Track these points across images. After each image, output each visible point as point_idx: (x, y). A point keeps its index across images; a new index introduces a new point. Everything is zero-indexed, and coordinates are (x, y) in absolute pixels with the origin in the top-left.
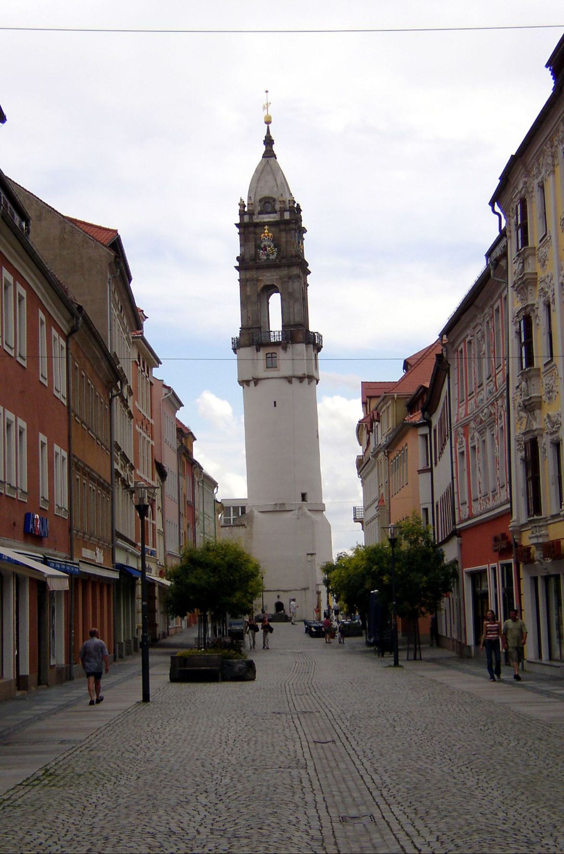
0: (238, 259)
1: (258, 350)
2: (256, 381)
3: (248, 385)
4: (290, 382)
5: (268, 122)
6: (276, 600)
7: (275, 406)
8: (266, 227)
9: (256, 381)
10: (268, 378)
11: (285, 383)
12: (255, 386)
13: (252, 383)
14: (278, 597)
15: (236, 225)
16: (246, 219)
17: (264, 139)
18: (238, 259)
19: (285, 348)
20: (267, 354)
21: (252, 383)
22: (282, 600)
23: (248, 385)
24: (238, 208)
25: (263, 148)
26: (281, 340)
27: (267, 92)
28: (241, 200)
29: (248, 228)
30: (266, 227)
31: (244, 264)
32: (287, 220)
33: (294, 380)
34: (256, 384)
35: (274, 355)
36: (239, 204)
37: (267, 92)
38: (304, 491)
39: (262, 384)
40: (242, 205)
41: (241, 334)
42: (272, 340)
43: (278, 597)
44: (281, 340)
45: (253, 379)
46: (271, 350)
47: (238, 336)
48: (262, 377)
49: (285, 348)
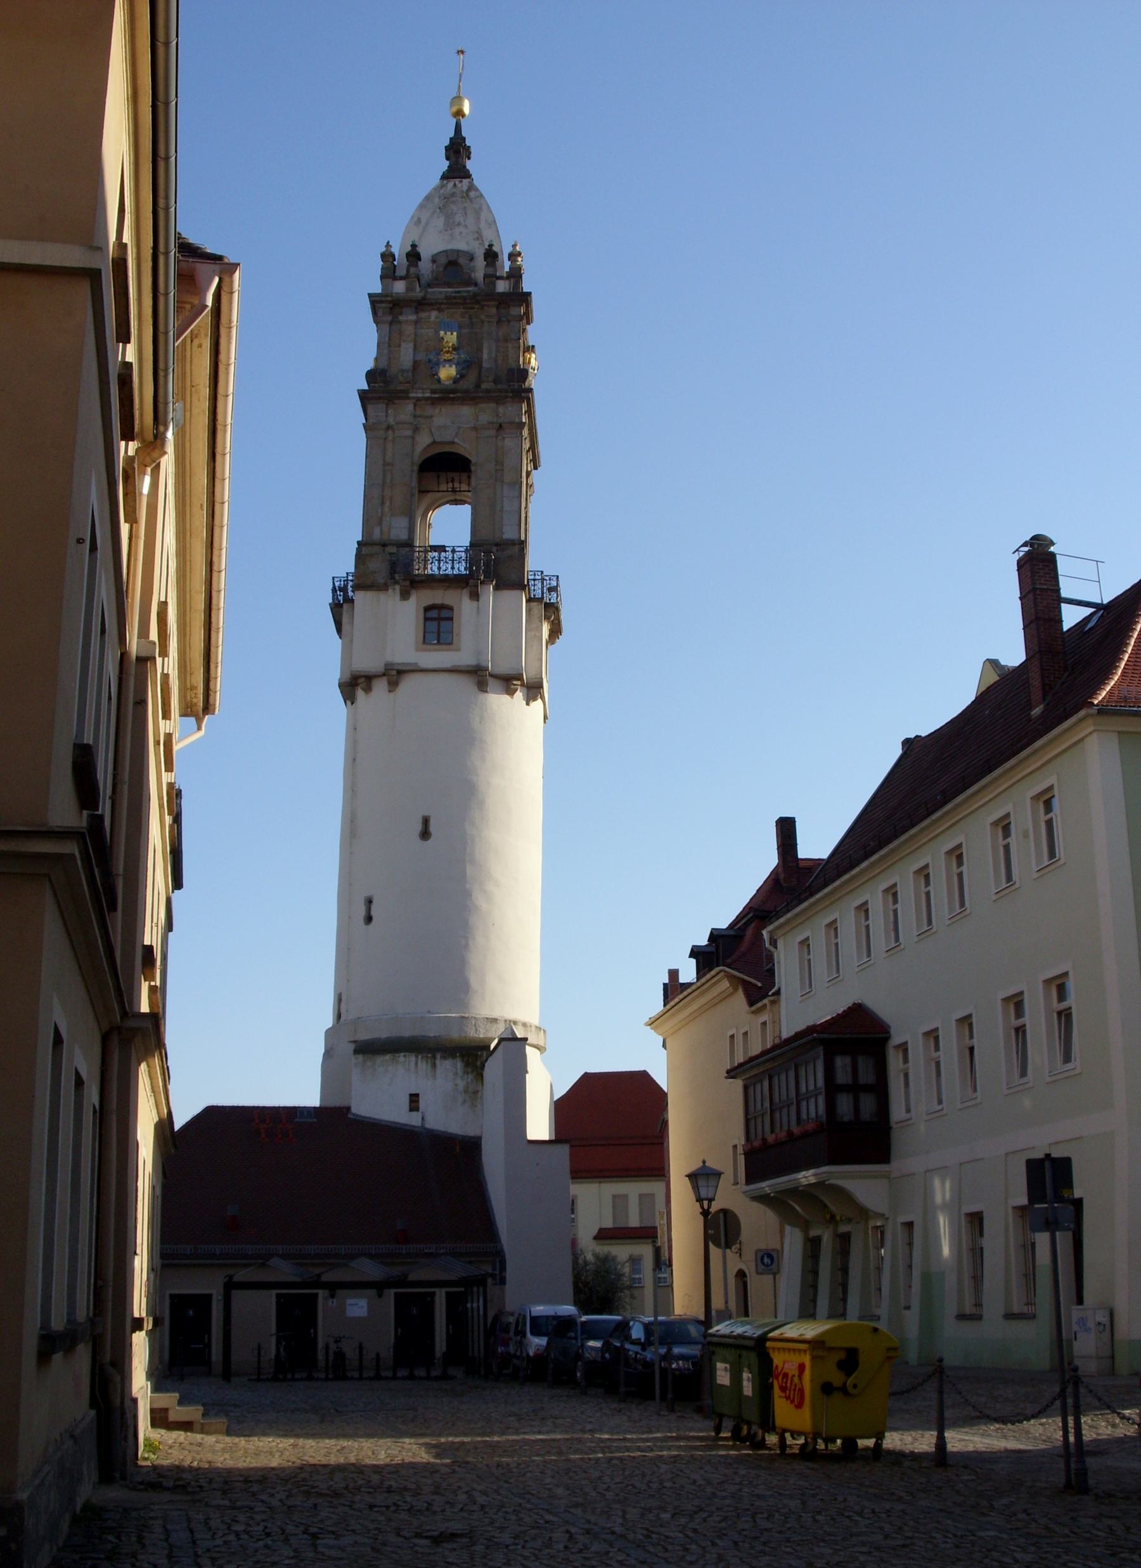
1: (405, 595)
2: (395, 675)
3: (368, 689)
9: (395, 675)
13: (380, 686)
15: (370, 295)
16: (399, 287)
17: (447, 143)
18: (371, 376)
20: (427, 609)
23: (368, 689)
24: (380, 263)
25: (444, 165)
28: (388, 245)
31: (380, 390)
32: (502, 294)
34: (393, 685)
41: (360, 558)
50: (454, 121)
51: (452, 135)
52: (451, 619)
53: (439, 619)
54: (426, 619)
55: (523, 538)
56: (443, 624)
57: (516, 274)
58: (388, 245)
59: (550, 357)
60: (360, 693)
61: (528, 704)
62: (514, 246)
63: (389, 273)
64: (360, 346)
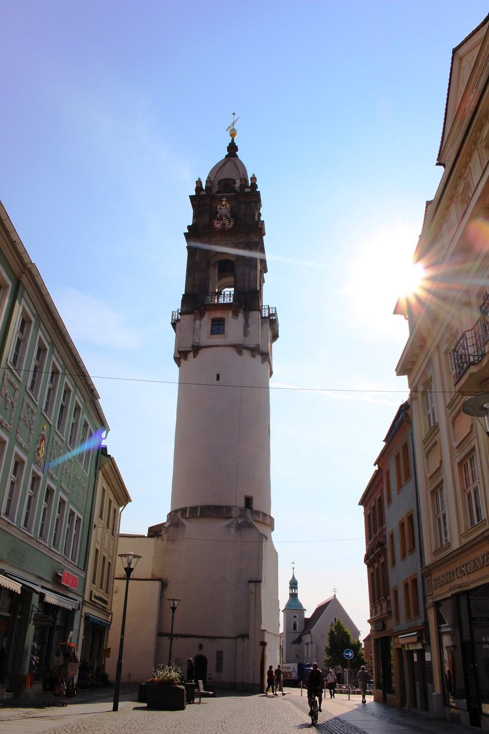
0: (189, 227)
1: (202, 316)
2: (196, 349)
4: (240, 353)
5: (233, 135)
6: (198, 652)
7: (218, 376)
8: (224, 199)
10: (211, 346)
11: (232, 351)
12: (194, 357)
13: (191, 355)
14: (201, 647)
18: (189, 227)
19: (235, 314)
21: (191, 355)
22: (204, 652)
23: (186, 358)
26: (232, 301)
27: (234, 114)
29: (202, 200)
30: (224, 199)
32: (248, 192)
33: (245, 352)
35: (220, 323)
36: (197, 182)
37: (234, 114)
38: (249, 494)
39: (203, 353)
40: (199, 182)
42: (221, 301)
43: (201, 647)
44: (232, 301)
45: (193, 347)
46: (218, 314)
47: (180, 307)
48: (204, 345)
49: (235, 314)
50: (231, 138)
51: (230, 142)
52: (224, 324)
53: (219, 325)
54: (212, 325)
55: (258, 289)
56: (220, 326)
57: (254, 186)
58: (199, 179)
59: (267, 213)
60: (183, 361)
61: (262, 363)
62: (254, 175)
63: (199, 188)
64: (186, 216)
